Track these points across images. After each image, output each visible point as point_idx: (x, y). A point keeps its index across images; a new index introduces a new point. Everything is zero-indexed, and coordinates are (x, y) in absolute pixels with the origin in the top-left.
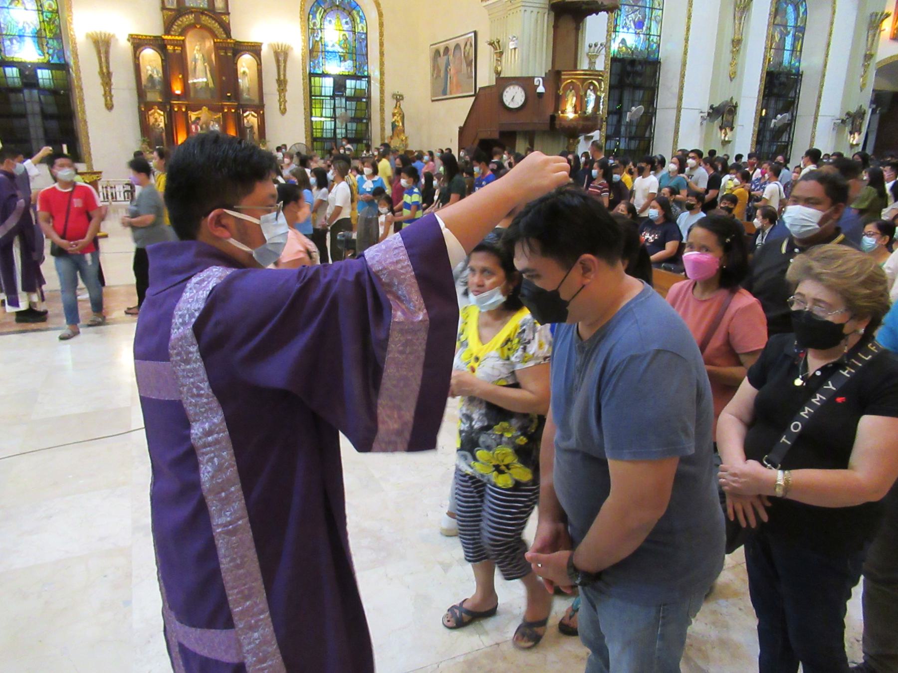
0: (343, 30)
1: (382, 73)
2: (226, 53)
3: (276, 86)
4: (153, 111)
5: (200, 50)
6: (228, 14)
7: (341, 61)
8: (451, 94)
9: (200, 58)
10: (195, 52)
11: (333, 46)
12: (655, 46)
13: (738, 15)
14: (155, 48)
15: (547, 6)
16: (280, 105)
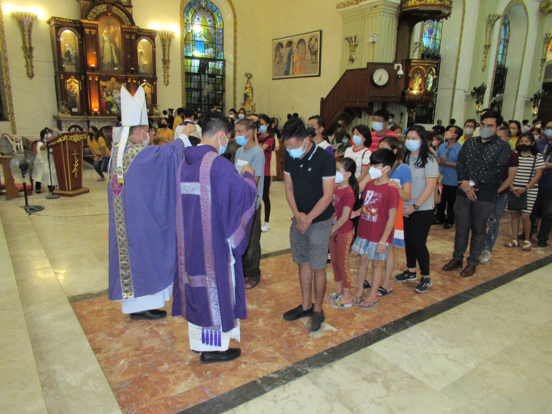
0: (208, 26)
1: (235, 58)
2: (130, 37)
3: (162, 65)
4: (70, 80)
5: (107, 34)
6: (131, 7)
7: (205, 48)
8: (293, 73)
9: (107, 40)
10: (104, 35)
11: (200, 37)
12: (438, 47)
13: (489, 29)
14: (74, 30)
15: (396, 13)
16: (165, 79)
